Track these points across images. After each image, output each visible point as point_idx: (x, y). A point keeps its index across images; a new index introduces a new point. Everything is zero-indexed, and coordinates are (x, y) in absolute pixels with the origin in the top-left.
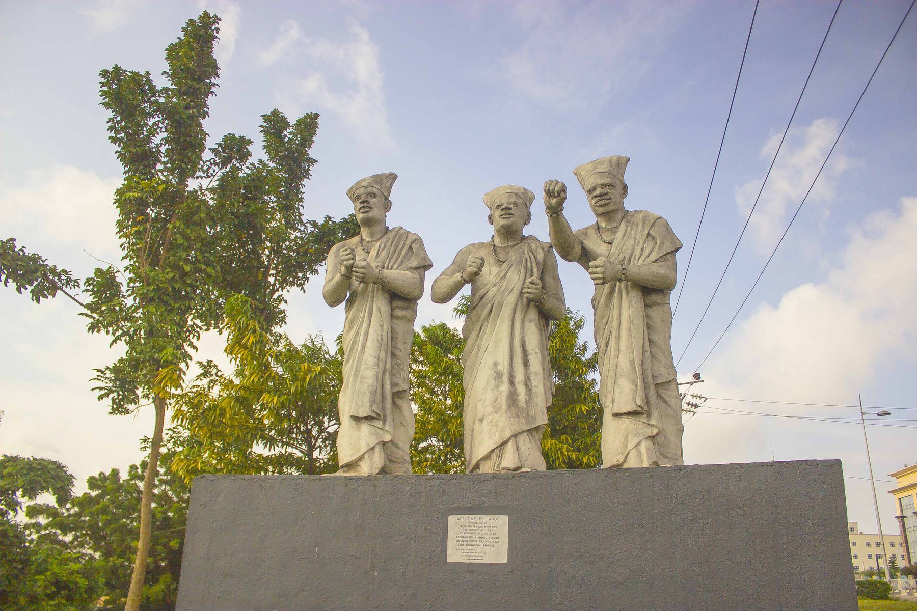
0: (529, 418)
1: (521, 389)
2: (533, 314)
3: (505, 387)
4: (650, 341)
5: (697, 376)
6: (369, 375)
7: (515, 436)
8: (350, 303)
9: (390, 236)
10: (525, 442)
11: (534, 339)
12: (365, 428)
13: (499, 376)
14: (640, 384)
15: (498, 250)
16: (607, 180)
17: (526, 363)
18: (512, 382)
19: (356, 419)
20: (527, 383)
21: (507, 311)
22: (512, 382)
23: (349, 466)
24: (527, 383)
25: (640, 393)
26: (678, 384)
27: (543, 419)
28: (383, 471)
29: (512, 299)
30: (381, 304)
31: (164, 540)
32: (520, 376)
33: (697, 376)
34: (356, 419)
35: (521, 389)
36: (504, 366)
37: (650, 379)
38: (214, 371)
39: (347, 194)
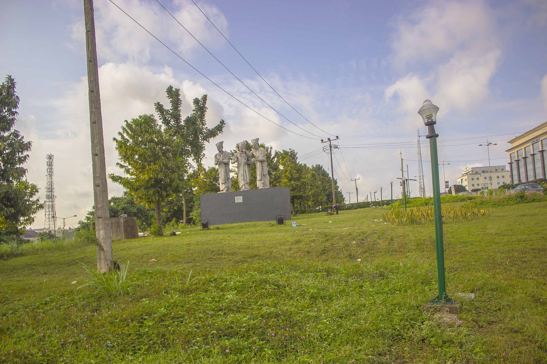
0: (246, 181)
1: (245, 177)
2: (246, 165)
3: (243, 177)
4: (263, 169)
5: (337, 137)
6: (223, 177)
7: (244, 184)
8: (219, 164)
9: (224, 153)
10: (246, 185)
11: (247, 169)
12: (223, 185)
13: (242, 175)
14: (260, 175)
15: (241, 154)
16: (255, 144)
17: (246, 173)
18: (244, 176)
19: (222, 184)
20: (246, 176)
21: (242, 165)
22: (244, 176)
23: (222, 191)
24: (246, 176)
25: (261, 177)
26: (330, 140)
27: (248, 181)
28: (227, 191)
29: (243, 163)
30: (224, 165)
31: (172, 207)
32: (245, 175)
33: (337, 137)
34: (222, 184)
35: (245, 177)
36: (242, 174)
37: (262, 175)
38: (190, 165)
39: (216, 145)
